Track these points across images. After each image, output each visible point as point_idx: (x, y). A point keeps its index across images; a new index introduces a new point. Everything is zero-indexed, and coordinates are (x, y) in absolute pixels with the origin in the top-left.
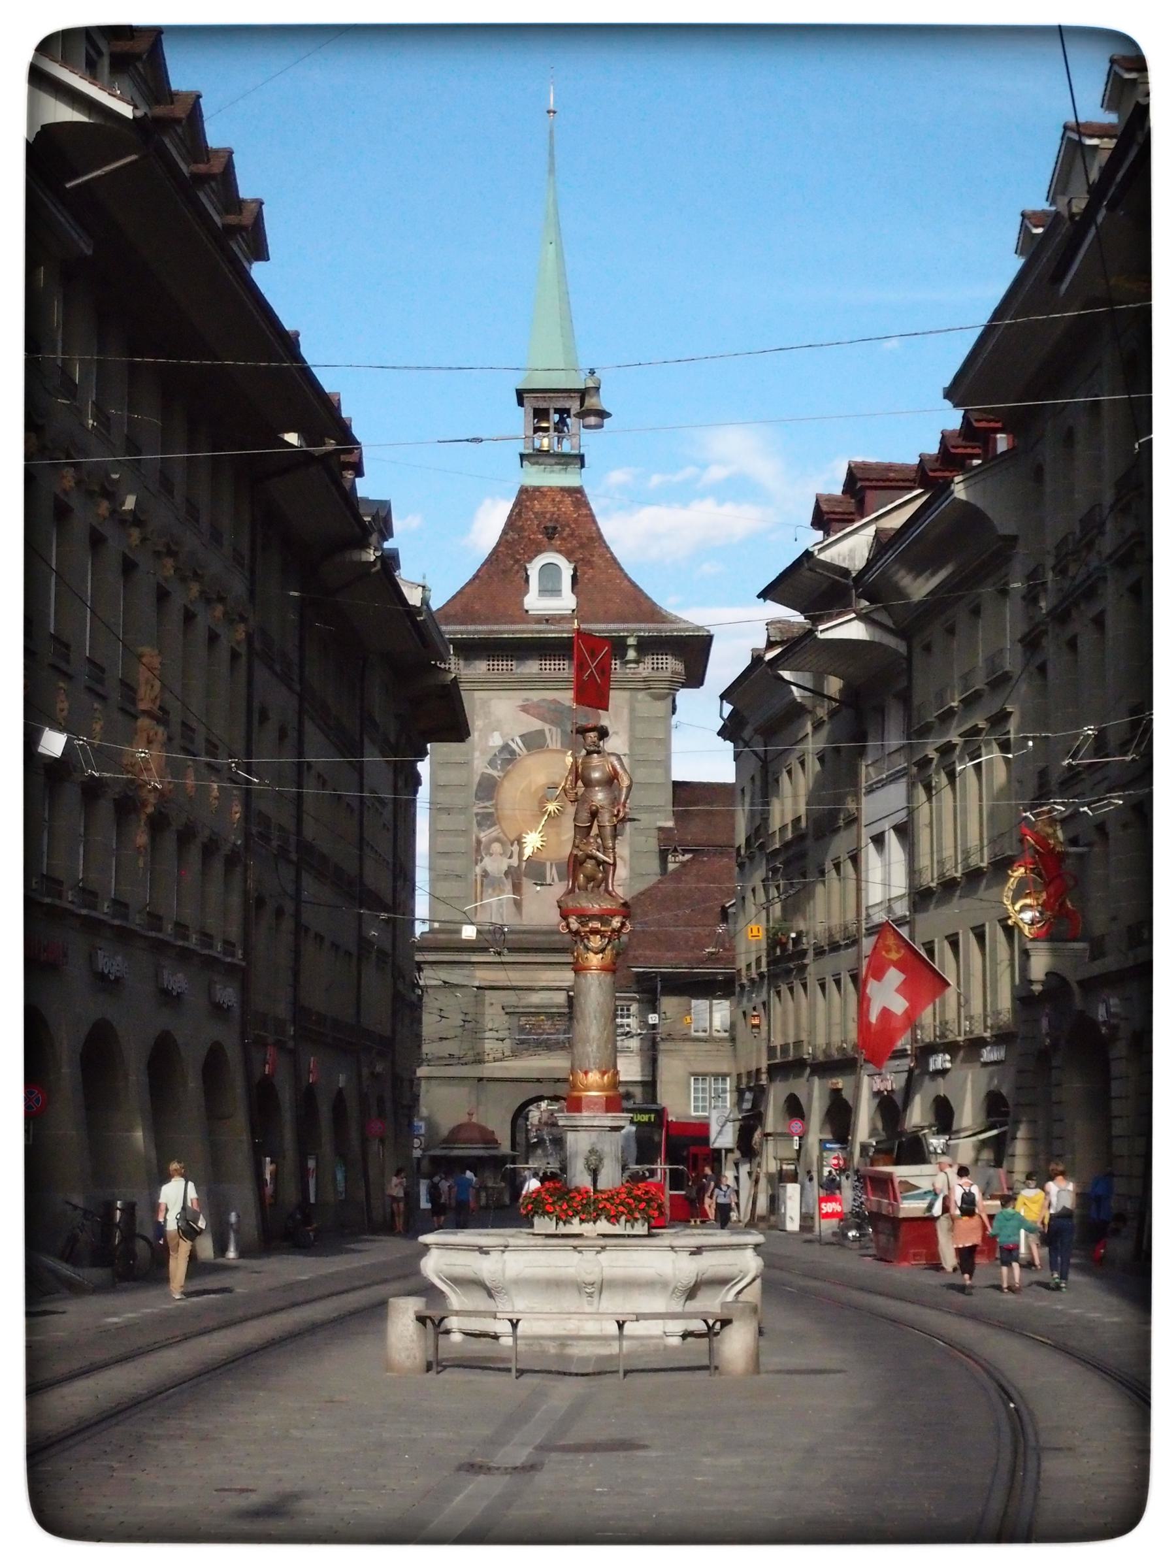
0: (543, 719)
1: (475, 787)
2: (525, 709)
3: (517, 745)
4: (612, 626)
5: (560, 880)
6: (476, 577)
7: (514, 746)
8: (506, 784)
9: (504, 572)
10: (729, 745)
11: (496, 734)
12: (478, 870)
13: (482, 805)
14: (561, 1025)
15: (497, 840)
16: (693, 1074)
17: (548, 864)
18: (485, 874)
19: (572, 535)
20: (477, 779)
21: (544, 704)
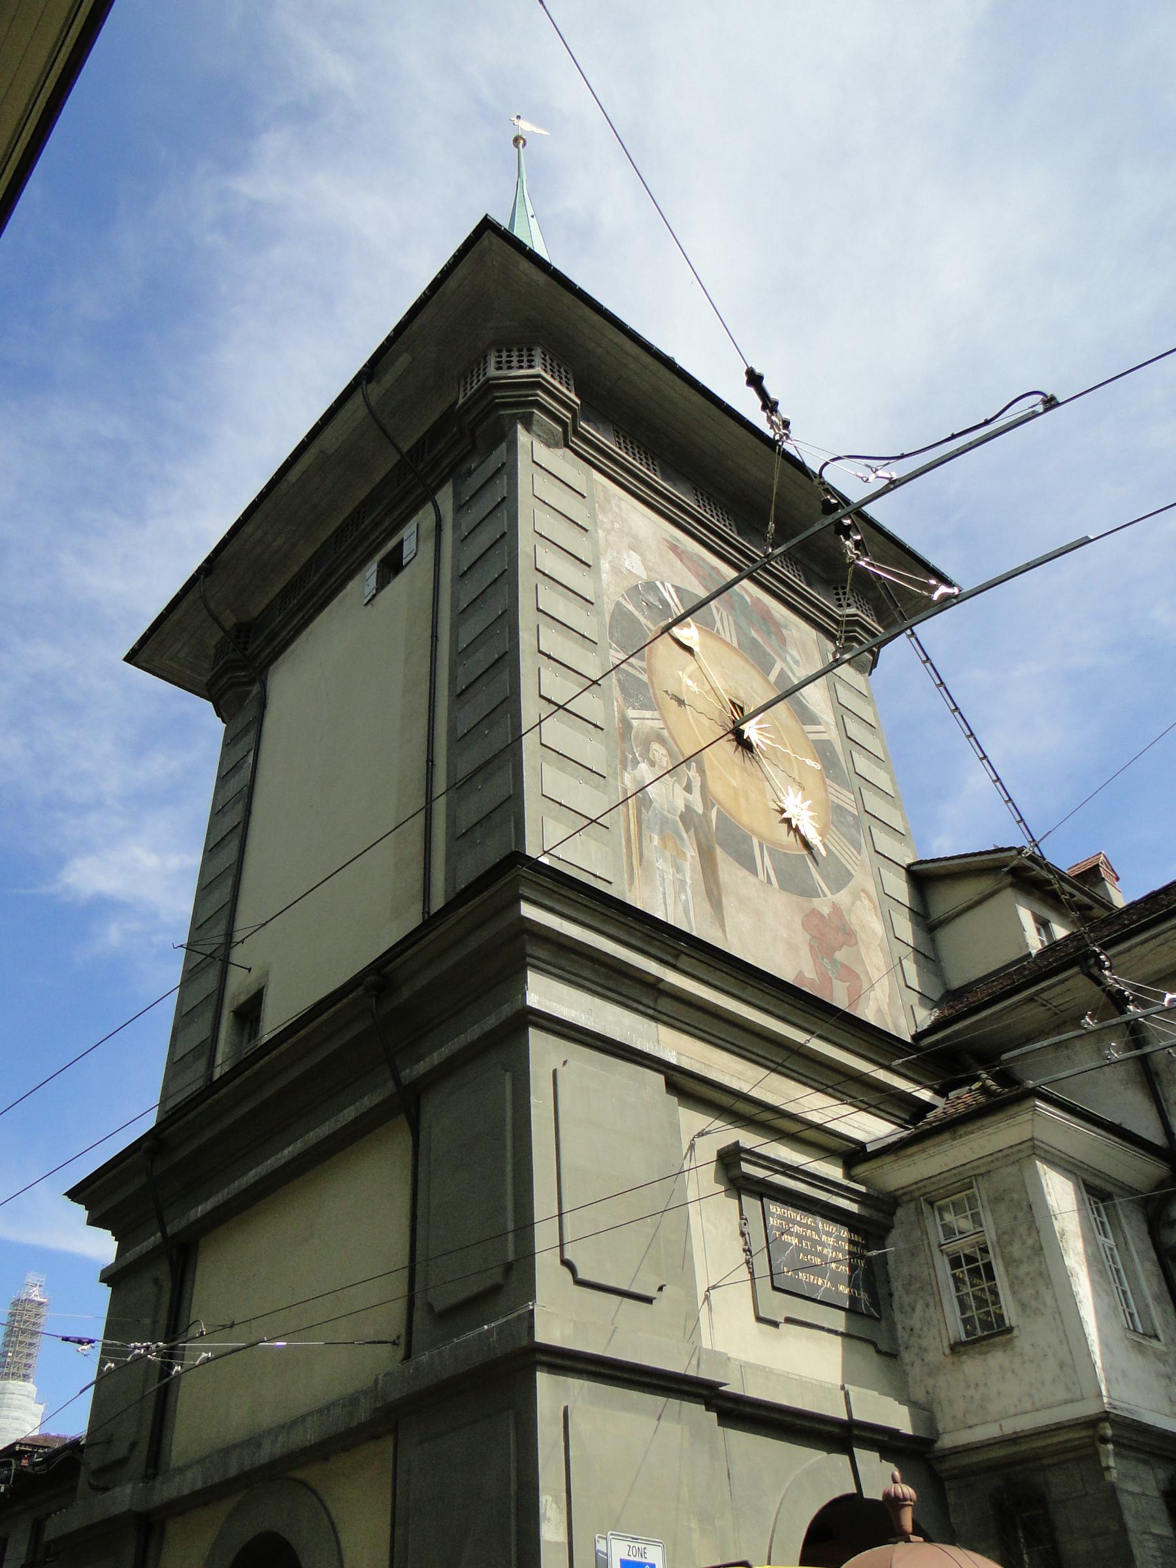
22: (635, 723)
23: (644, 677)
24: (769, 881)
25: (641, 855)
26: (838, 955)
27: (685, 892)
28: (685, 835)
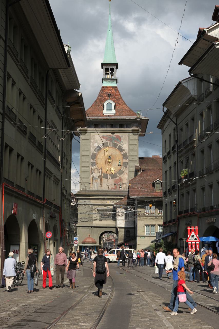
2: (103, 137)
3: (101, 146)
4: (124, 117)
5: (111, 178)
6: (92, 107)
7: (100, 146)
8: (98, 155)
9: (98, 106)
10: (160, 130)
11: (96, 143)
12: (92, 176)
13: (93, 160)
15: (96, 169)
16: (146, 225)
18: (93, 177)
19: (114, 97)
20: (91, 154)
21: (107, 136)
22: (93, 169)
24: (110, 179)
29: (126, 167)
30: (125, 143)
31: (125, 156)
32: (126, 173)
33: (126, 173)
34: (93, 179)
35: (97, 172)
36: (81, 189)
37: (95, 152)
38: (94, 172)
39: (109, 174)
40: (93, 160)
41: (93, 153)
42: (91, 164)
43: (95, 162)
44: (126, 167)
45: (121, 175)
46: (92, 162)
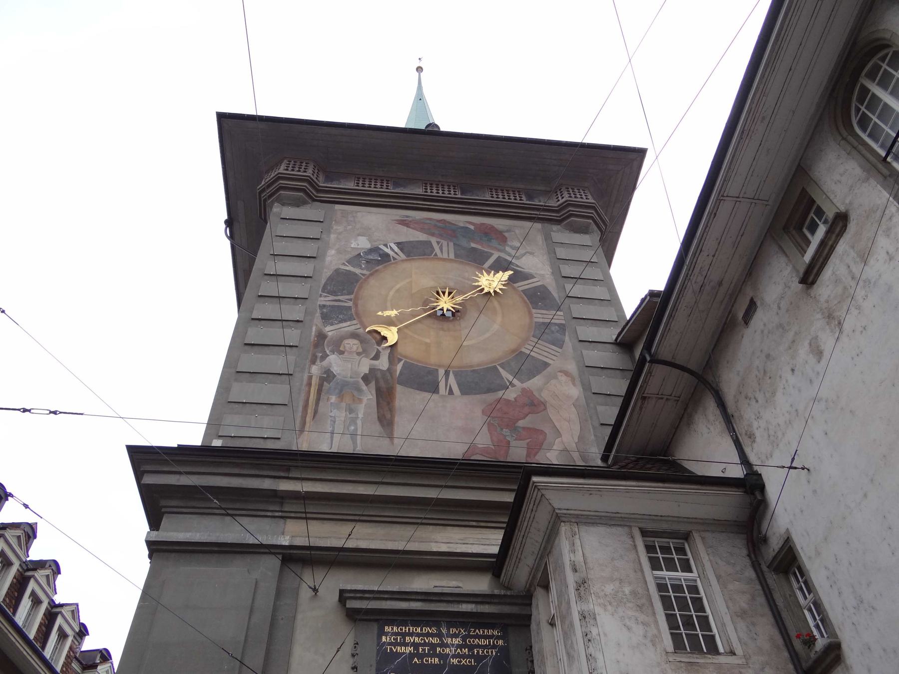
0: (433, 235)
1: (323, 281)
2: (403, 222)
3: (392, 249)
7: (388, 251)
8: (372, 281)
12: (315, 370)
14: (487, 642)
15: (354, 335)
17: (441, 372)
18: (328, 376)
20: (327, 273)
22: (330, 334)
23: (350, 304)
24: (451, 392)
25: (316, 412)
26: (521, 423)
27: (356, 424)
28: (364, 388)
29: (560, 344)
30: (532, 253)
31: (538, 298)
32: (566, 373)
33: (566, 373)
34: (320, 386)
35: (359, 354)
36: (217, 443)
37: (349, 268)
38: (333, 352)
39: (440, 366)
40: (331, 298)
41: (337, 272)
42: (318, 314)
43: (346, 304)
44: (560, 344)
45: (530, 379)
46: (328, 303)
